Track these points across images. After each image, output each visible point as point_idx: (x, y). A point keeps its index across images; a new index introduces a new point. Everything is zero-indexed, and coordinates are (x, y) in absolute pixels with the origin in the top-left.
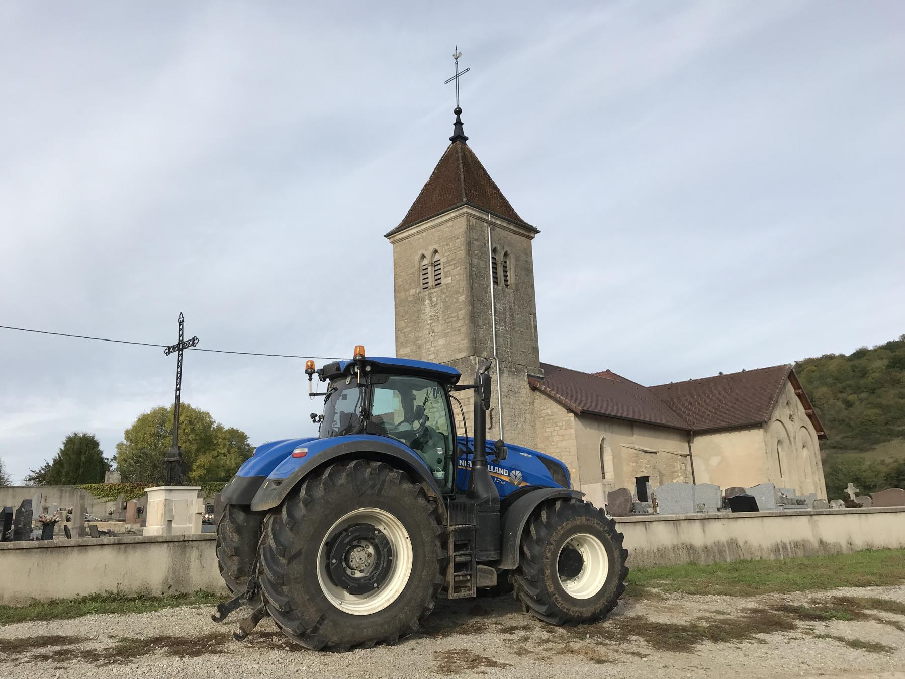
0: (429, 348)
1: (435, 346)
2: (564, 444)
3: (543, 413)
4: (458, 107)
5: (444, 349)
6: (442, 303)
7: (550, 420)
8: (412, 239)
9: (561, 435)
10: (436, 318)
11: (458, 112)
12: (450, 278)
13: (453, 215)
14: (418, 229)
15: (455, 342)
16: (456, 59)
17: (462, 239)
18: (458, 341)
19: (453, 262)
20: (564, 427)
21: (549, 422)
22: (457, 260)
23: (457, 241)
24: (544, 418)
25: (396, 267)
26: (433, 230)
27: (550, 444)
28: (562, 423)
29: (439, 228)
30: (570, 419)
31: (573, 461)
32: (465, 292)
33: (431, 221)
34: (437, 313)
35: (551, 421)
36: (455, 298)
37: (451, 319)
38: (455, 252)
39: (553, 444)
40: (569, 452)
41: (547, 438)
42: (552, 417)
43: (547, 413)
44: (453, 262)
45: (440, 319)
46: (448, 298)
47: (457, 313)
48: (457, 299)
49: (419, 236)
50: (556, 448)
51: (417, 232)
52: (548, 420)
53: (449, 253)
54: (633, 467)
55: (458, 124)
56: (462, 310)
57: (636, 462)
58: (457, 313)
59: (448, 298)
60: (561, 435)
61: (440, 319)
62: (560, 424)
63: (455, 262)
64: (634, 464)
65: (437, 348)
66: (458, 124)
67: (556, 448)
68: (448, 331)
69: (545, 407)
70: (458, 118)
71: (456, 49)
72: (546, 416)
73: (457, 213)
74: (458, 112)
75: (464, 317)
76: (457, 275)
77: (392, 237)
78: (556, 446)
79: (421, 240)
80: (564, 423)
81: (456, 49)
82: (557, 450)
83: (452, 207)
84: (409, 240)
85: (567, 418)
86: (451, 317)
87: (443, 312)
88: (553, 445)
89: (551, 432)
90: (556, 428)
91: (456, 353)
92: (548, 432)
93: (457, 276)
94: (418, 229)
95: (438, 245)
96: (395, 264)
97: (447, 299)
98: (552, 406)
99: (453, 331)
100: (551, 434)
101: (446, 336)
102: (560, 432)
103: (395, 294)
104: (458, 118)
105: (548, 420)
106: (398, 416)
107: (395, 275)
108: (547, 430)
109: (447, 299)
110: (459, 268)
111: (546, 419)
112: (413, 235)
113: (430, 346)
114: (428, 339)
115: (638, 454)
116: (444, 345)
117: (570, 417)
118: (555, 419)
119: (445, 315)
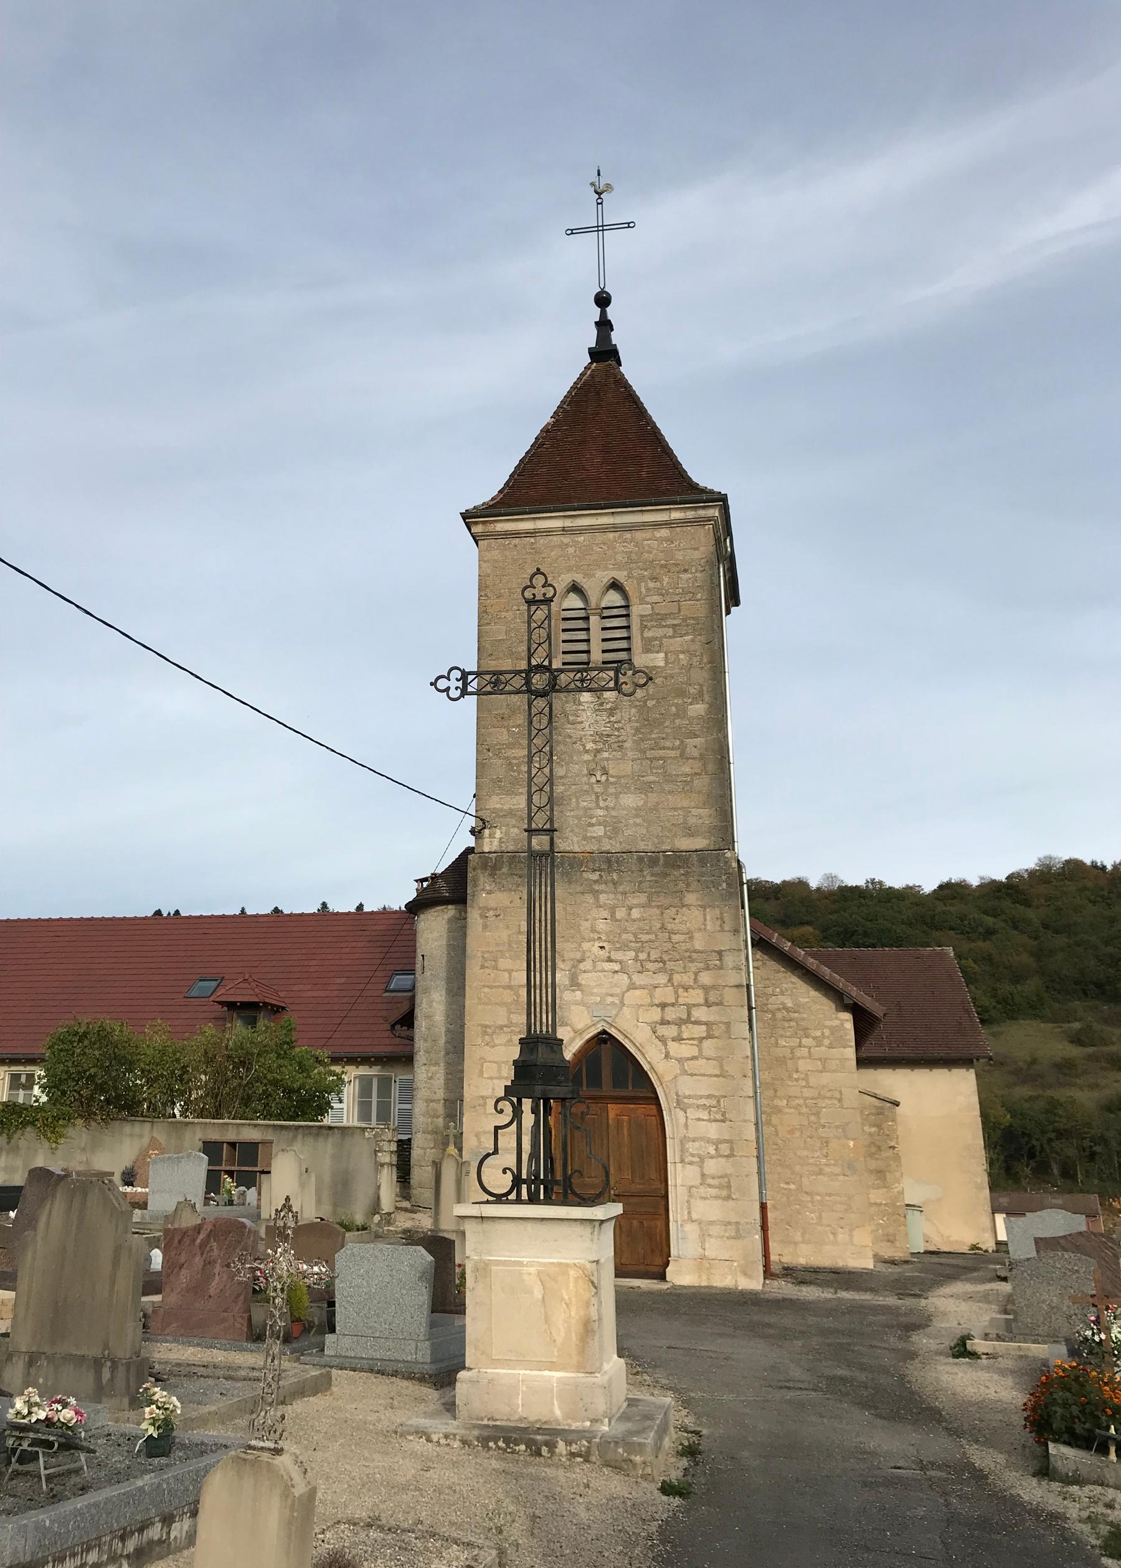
0: (586, 809)
1: (607, 808)
2: (825, 1079)
3: (771, 1000)
4: (603, 291)
5: (638, 821)
6: (634, 710)
7: (791, 1020)
8: (542, 541)
9: (820, 1059)
10: (611, 740)
11: (603, 300)
12: (662, 655)
13: (676, 515)
14: (568, 523)
15: (675, 809)
16: (599, 194)
17: (698, 575)
18: (682, 808)
19: (669, 622)
20: (826, 1042)
21: (786, 1024)
22: (684, 620)
23: (684, 576)
24: (774, 1014)
25: (486, 595)
26: (611, 535)
27: (790, 1077)
28: (823, 1034)
29: (628, 535)
30: (842, 1025)
31: (847, 1124)
32: (706, 697)
33: (613, 513)
34: (618, 729)
35: (792, 1024)
36: (676, 705)
37: (661, 753)
38: (677, 598)
39: (795, 1076)
40: (840, 1100)
41: (781, 1061)
42: (797, 1015)
43: (782, 1003)
44: (669, 622)
45: (627, 745)
46: (654, 702)
47: (682, 742)
48: (681, 713)
49: (566, 540)
50: (805, 1087)
51: (564, 529)
52: (784, 1019)
53: (656, 598)
54: (870, 1134)
55: (604, 325)
56: (696, 736)
57: (879, 1126)
58: (682, 742)
59: (654, 702)
60: (820, 1059)
61: (626, 745)
62: (818, 1033)
63: (675, 622)
64: (873, 1130)
65: (614, 813)
66: (604, 325)
67: (805, 1087)
68: (652, 778)
69: (778, 990)
70: (603, 314)
71: (599, 175)
72: (779, 1009)
73: (690, 514)
74: (603, 300)
75: (701, 755)
76: (683, 652)
77: (484, 523)
78: (804, 1083)
79: (571, 550)
80: (827, 1032)
81: (599, 175)
82: (807, 1093)
83: (685, 497)
84: (532, 540)
85: (837, 1023)
86: (664, 748)
87: (637, 730)
88: (797, 1080)
89: (792, 1049)
90: (804, 1041)
91: (675, 835)
92: (785, 1046)
93: (682, 656)
94: (568, 523)
95: (625, 573)
96: (482, 587)
97: (650, 703)
98: (795, 988)
99: (667, 781)
100: (792, 1053)
101: (646, 789)
102: (818, 1051)
103: (479, 659)
104: (603, 314)
105: (784, 1019)
106: (482, 967)
107: (483, 612)
108: (782, 1042)
109: (650, 703)
110: (686, 638)
111: (779, 1015)
112: (548, 532)
113: (593, 805)
114: (586, 787)
115: (882, 1108)
116: (638, 809)
117: (843, 1021)
118: (803, 1019)
119: (643, 740)
